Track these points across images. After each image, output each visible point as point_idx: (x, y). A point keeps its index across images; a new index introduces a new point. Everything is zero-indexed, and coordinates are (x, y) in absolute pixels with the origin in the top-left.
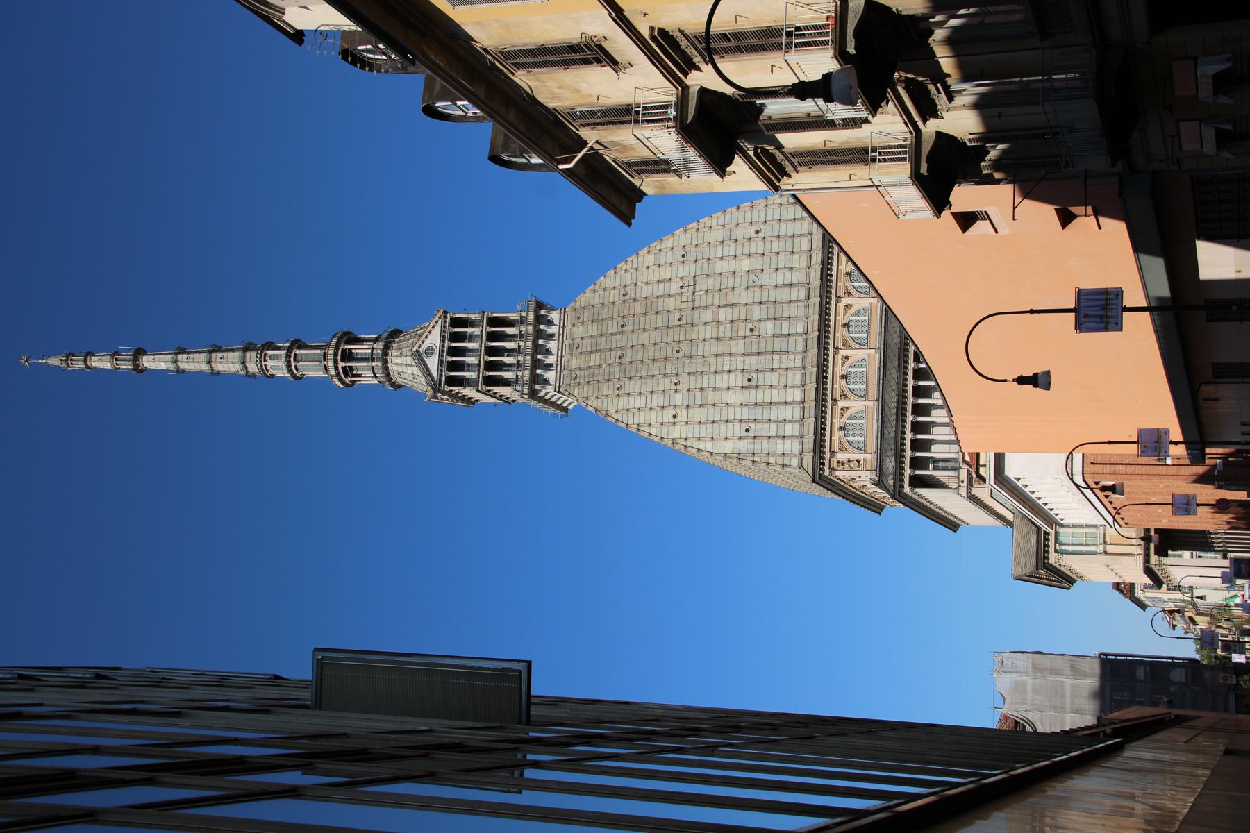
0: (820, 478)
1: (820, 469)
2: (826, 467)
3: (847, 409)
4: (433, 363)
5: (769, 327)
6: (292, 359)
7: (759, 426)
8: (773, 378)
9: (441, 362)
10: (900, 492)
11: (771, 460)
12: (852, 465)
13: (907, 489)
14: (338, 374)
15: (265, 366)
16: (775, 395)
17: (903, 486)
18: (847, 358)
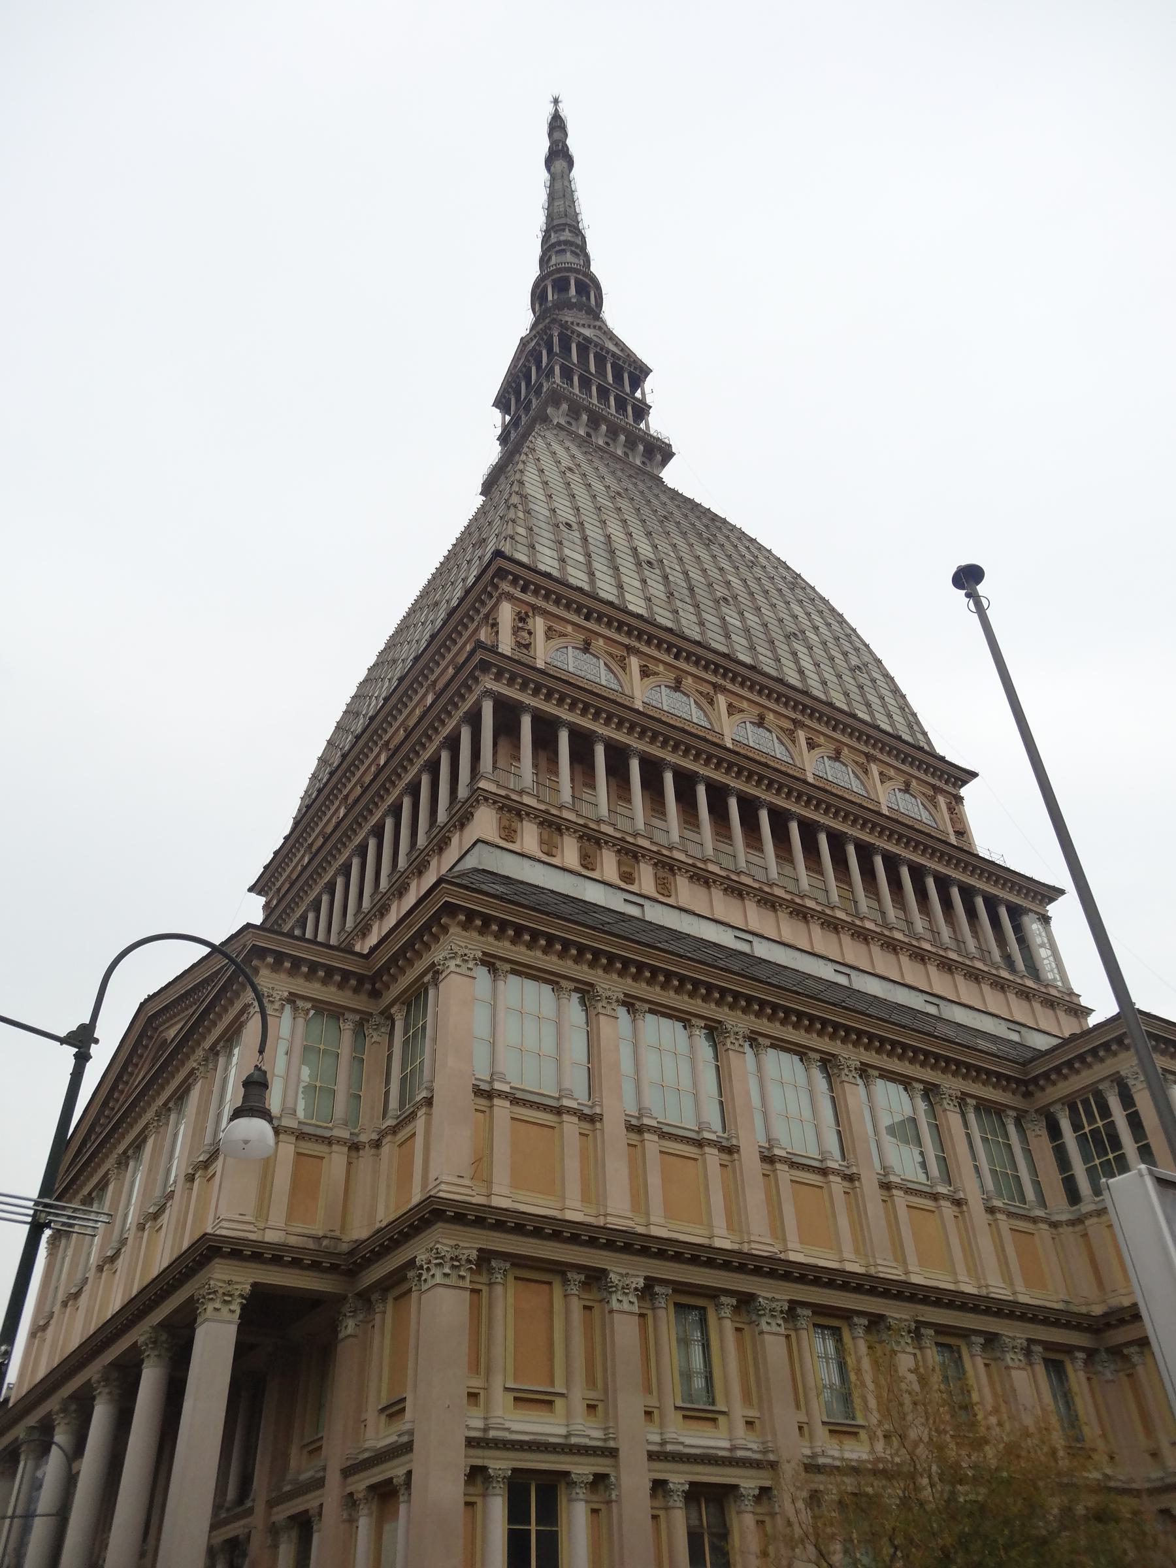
0: (500, 569)
1: (516, 578)
2: (518, 593)
3: (624, 669)
4: (587, 332)
5: (733, 621)
6: (573, 249)
7: (578, 541)
8: (657, 589)
9: (586, 338)
10: (484, 666)
11: (521, 531)
12: (525, 634)
13: (488, 682)
14: (559, 270)
15: (564, 230)
16: (631, 580)
17: (498, 677)
18: (711, 702)
